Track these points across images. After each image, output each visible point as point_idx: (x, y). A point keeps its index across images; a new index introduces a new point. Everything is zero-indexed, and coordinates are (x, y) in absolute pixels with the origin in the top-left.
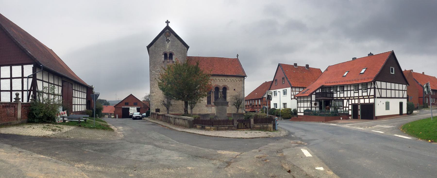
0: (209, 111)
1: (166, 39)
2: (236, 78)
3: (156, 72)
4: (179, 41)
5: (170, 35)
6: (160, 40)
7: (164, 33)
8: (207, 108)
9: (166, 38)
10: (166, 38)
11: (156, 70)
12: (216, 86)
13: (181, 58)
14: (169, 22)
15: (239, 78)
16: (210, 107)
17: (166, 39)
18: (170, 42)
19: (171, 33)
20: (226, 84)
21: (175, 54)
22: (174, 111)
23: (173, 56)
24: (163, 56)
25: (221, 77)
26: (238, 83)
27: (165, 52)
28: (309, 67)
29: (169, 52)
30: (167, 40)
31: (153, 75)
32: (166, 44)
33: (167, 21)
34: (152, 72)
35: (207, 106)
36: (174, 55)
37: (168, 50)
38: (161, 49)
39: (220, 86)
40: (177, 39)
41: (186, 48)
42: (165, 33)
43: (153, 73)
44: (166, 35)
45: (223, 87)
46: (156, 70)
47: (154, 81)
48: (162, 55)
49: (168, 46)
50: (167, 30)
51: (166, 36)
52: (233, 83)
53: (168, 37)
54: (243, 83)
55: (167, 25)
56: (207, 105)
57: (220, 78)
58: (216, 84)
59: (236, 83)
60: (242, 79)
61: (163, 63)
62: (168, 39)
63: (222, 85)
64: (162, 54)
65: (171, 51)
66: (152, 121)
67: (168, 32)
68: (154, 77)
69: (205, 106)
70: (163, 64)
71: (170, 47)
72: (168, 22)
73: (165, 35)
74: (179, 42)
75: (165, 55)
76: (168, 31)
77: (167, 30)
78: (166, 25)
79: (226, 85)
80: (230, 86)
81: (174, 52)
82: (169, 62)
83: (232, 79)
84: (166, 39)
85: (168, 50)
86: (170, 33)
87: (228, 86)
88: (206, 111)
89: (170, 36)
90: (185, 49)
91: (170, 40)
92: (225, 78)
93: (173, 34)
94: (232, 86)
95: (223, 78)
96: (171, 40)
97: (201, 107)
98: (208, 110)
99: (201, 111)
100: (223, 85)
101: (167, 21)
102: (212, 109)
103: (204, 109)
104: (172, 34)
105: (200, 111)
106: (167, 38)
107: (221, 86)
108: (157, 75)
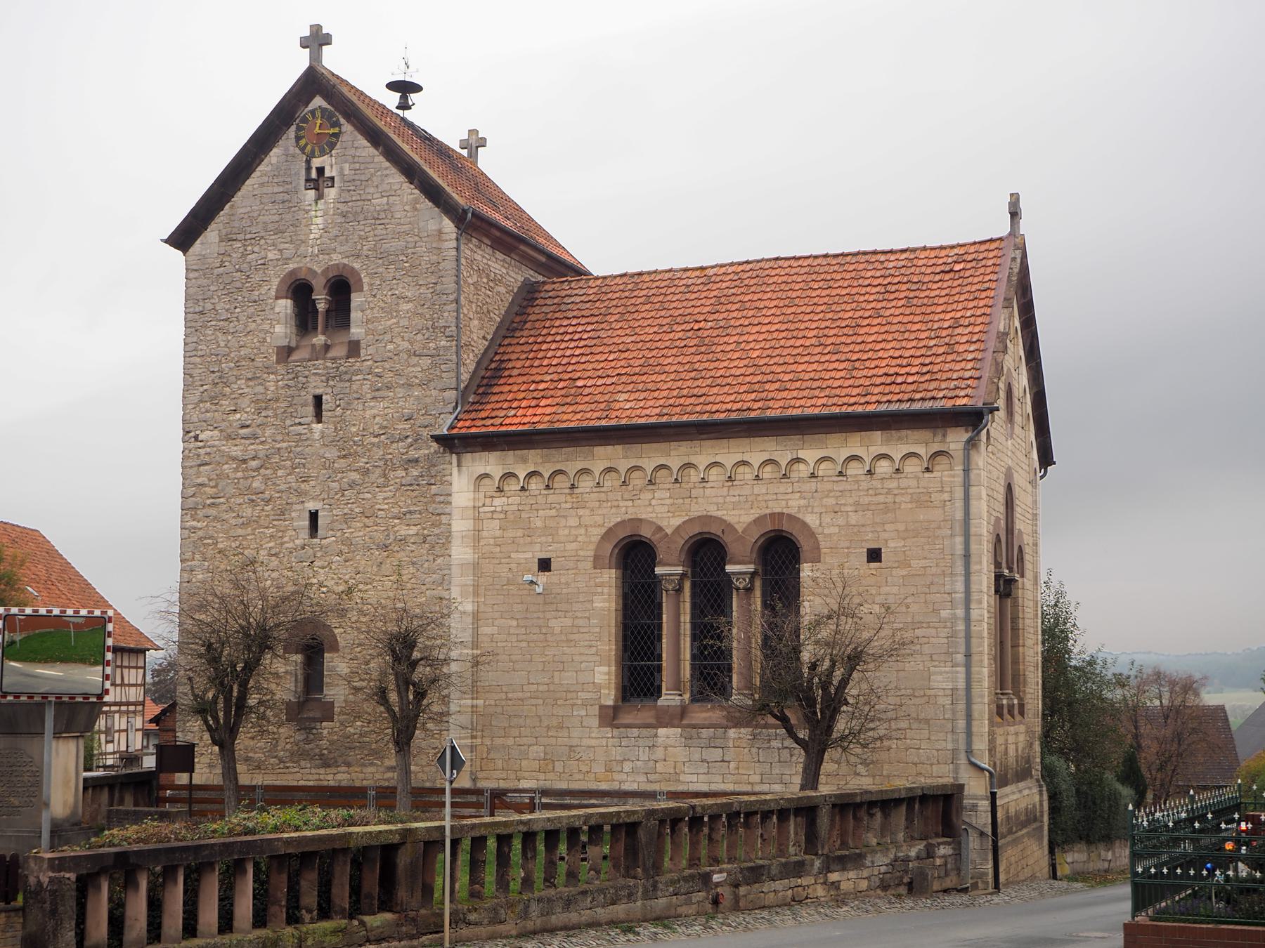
0: (627, 767)
1: (308, 169)
2: (887, 442)
3: (229, 437)
4: (394, 170)
5: (336, 135)
6: (262, 185)
7: (293, 128)
8: (608, 732)
9: (308, 162)
10: (308, 162)
11: (223, 425)
12: (715, 530)
13: (410, 305)
14: (326, 40)
15: (925, 434)
16: (635, 732)
17: (308, 169)
18: (331, 193)
19: (342, 121)
20: (793, 505)
21: (365, 280)
22: (349, 765)
23: (353, 295)
24: (285, 306)
25: (816, 436)
26: (913, 483)
27: (293, 272)
28: (308, 34)
29: (323, 272)
30: (314, 175)
31: (207, 464)
32: (307, 212)
33: (316, 29)
34: (196, 438)
35: (610, 717)
36: (361, 290)
37: (322, 252)
38: (271, 256)
39: (730, 525)
40: (381, 158)
41: (450, 219)
42: (299, 129)
43: (202, 451)
44: (303, 142)
45: (755, 534)
46: (223, 425)
47: (213, 512)
48: (277, 298)
49: (319, 220)
50: (318, 102)
51: (303, 150)
52: (864, 485)
53: (323, 153)
54: (959, 479)
55: (307, 65)
56: (616, 709)
57: (729, 453)
58: (696, 510)
59: (889, 491)
60: (956, 439)
61: (278, 362)
62: (321, 171)
63: (750, 518)
64: (273, 293)
65: (336, 259)
66: (290, 814)
67: (318, 114)
68: (210, 480)
69: (595, 722)
70: (281, 369)
71: (334, 232)
72: (317, 40)
73: (298, 139)
74: (396, 178)
75: (300, 291)
76: (324, 104)
77: (318, 102)
78: (300, 62)
79: (793, 511)
80: (827, 519)
81: (356, 266)
82: (327, 348)
83: (845, 453)
84: (303, 172)
85: (322, 252)
86: (337, 124)
87: (811, 520)
88: (599, 768)
89: (332, 146)
90: (440, 232)
91: (332, 179)
92: (779, 450)
93: (354, 125)
94: (853, 519)
95: (757, 451)
96: (342, 174)
97: (560, 727)
98: (617, 753)
99: (559, 766)
100: (757, 521)
101: (316, 29)
102: (659, 753)
103: (586, 742)
104: (347, 127)
105: (548, 761)
106: (316, 162)
107: (740, 528)
108: (234, 459)
